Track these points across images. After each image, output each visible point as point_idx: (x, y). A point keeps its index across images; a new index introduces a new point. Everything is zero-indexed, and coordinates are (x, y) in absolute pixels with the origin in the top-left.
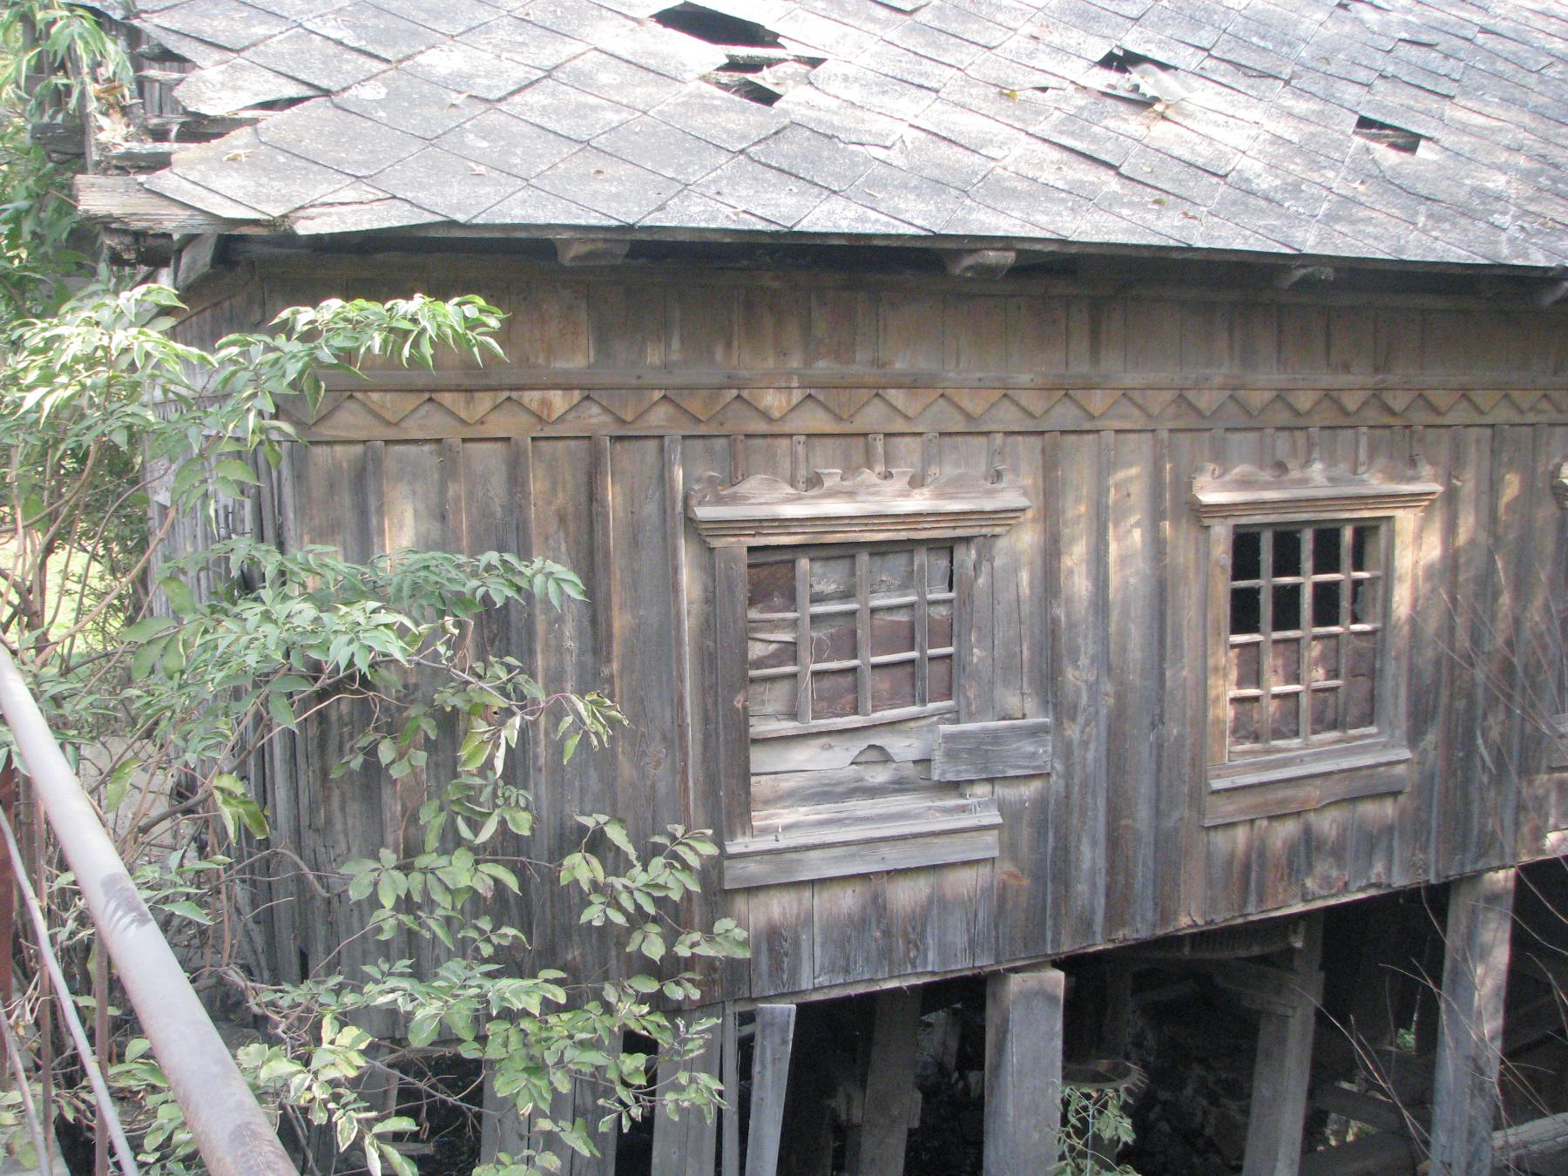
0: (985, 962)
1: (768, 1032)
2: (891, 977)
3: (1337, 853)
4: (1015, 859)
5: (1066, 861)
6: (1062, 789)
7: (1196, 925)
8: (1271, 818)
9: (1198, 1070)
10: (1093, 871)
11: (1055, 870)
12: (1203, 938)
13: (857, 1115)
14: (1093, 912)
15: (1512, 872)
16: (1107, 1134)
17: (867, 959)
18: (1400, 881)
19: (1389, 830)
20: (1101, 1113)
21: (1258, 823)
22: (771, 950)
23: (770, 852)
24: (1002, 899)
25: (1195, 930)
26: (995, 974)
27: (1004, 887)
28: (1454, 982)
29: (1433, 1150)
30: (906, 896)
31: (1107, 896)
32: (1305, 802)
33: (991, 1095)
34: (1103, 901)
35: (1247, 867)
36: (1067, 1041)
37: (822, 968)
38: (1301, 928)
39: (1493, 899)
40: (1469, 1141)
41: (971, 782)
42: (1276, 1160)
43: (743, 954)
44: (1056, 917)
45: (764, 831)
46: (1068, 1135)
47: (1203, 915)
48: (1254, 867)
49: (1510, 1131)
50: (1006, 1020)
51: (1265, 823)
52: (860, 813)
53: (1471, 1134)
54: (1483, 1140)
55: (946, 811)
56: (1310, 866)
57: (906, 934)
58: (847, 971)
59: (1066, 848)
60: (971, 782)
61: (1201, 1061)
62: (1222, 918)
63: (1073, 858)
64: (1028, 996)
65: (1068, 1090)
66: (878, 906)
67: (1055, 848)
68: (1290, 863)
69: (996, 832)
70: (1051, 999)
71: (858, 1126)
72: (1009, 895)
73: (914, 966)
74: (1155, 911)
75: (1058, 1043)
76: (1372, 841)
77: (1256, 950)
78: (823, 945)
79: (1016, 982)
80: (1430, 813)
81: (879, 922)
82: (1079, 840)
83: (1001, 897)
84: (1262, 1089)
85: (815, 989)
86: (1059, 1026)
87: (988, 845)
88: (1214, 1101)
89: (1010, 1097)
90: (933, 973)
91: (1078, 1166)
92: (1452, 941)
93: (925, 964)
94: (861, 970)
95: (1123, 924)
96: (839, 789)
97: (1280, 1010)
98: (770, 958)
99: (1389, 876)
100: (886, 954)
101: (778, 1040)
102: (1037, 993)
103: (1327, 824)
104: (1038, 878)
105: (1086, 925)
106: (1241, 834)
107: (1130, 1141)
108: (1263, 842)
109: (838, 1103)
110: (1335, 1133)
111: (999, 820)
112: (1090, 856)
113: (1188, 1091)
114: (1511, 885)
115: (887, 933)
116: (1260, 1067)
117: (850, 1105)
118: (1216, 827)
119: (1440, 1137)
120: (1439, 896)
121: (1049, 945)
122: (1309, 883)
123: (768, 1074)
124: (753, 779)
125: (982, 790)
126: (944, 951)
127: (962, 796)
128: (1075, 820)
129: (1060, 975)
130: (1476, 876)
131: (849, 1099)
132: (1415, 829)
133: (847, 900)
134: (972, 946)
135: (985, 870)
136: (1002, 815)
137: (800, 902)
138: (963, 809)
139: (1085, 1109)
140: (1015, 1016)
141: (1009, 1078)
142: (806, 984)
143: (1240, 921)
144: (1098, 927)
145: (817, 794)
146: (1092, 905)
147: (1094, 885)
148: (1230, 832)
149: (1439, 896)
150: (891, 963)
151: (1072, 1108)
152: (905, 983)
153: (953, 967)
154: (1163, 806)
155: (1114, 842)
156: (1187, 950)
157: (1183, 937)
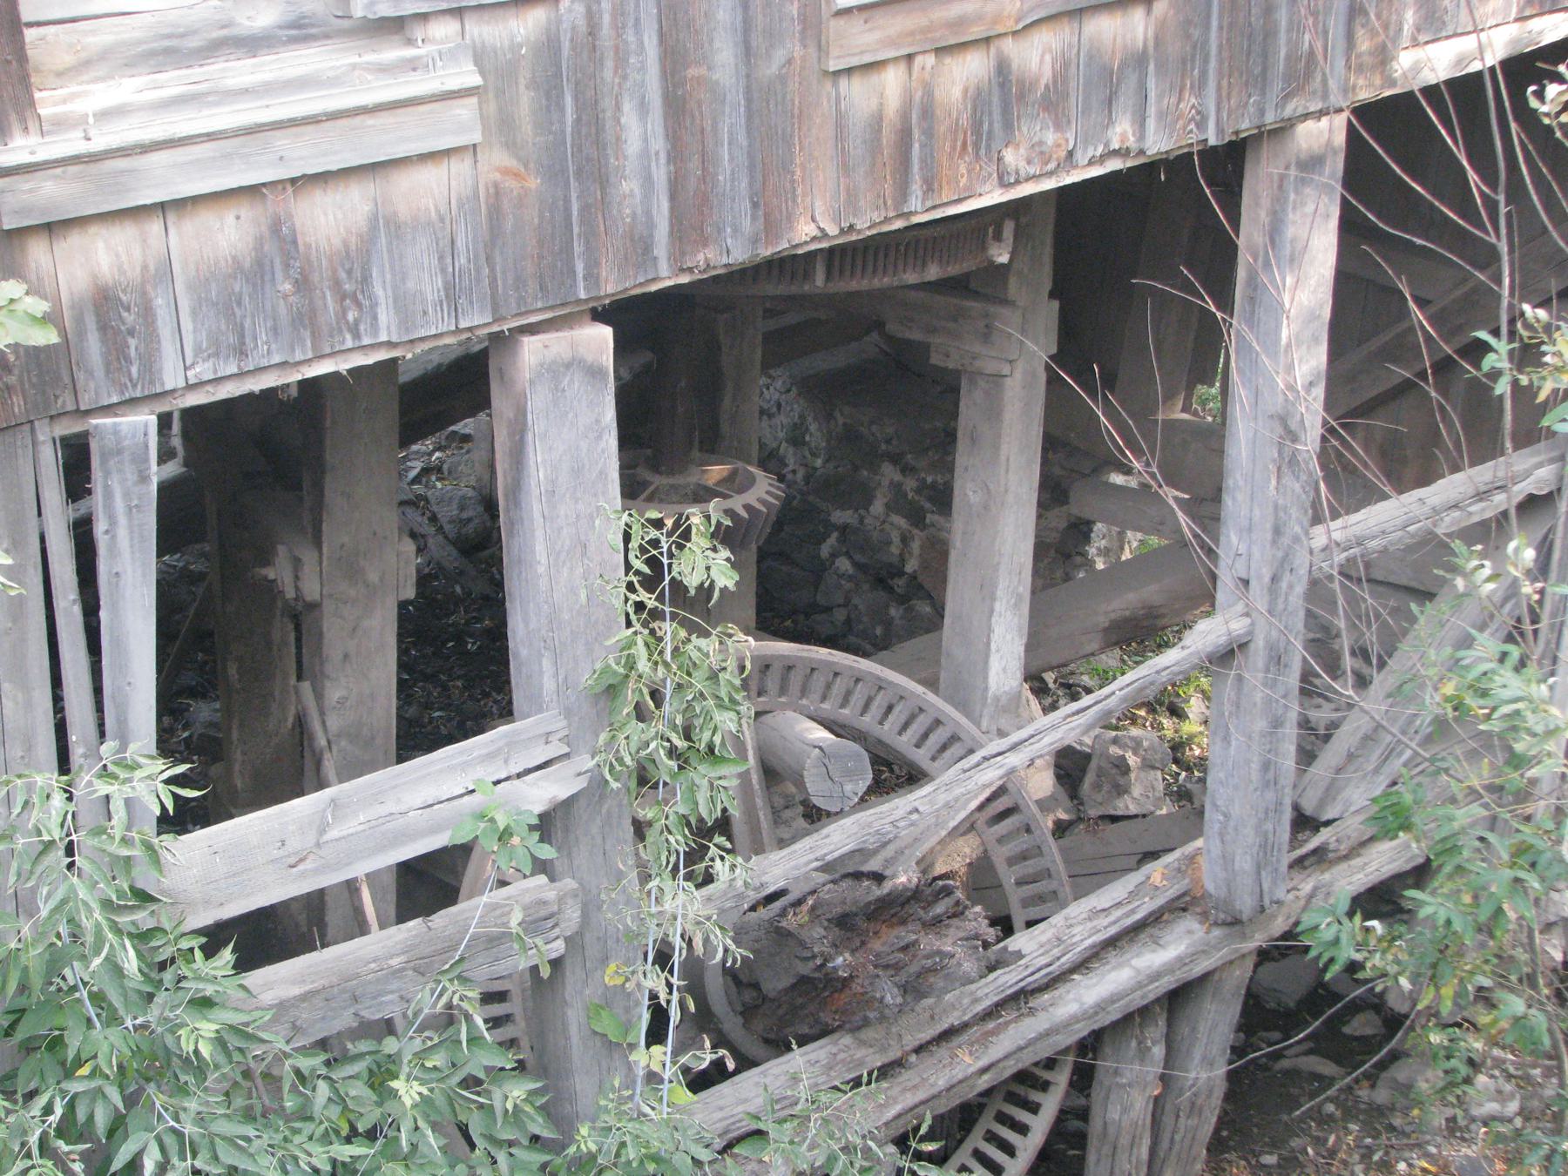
0: (477, 318)
2: (320, 357)
3: (1053, 103)
4: (511, 146)
5: (599, 144)
6: (581, 23)
7: (825, 235)
8: (940, 51)
9: (889, 472)
10: (645, 154)
11: (582, 158)
12: (844, 256)
13: (311, 589)
14: (651, 225)
15: (1340, 121)
16: (692, 581)
17: (275, 330)
18: (1158, 143)
19: (1139, 60)
20: (681, 547)
21: (919, 60)
22: (103, 328)
23: (76, 160)
24: (495, 213)
25: (824, 245)
26: (496, 337)
27: (497, 192)
28: (1252, 300)
29: (1222, 564)
30: (327, 220)
31: (673, 197)
32: (997, 19)
33: (511, 534)
34: (666, 205)
35: (905, 135)
36: (625, 441)
37: (198, 350)
38: (1009, 229)
39: (1312, 163)
40: (1274, 542)
41: (424, 17)
42: (993, 599)
43: (47, 337)
44: (590, 236)
45: (61, 124)
46: (630, 587)
47: (837, 219)
48: (916, 134)
49: (1334, 525)
50: (521, 412)
51: (930, 60)
52: (232, 82)
53: (1277, 531)
54: (1296, 539)
55: (383, 69)
56: (1008, 126)
57: (337, 284)
58: (241, 352)
59: (598, 123)
60: (424, 17)
61: (895, 459)
62: (868, 221)
63: (609, 136)
64: (555, 371)
65: (625, 517)
66: (283, 238)
67: (578, 121)
68: (977, 126)
69: (474, 100)
70: (594, 372)
71: (314, 607)
72: (506, 205)
73: (357, 336)
74: (754, 218)
75: (611, 441)
76: (1108, 82)
77: (933, 272)
78: (194, 313)
79: (532, 351)
80: (1207, 26)
81: (287, 266)
82: (618, 107)
83: (494, 209)
84: (967, 492)
85: (190, 387)
86: (610, 414)
87: (461, 124)
88: (917, 518)
89: (539, 533)
90: (390, 345)
91: (653, 632)
92: (1250, 236)
94: (266, 351)
95: (705, 242)
96: (194, 43)
97: (990, 367)
98: (104, 341)
99: (1141, 136)
100: (306, 319)
101: (131, 476)
102: (568, 366)
103: (1035, 56)
104: (554, 173)
105: (641, 248)
106: (892, 81)
107: (731, 585)
108: (929, 92)
109: (279, 572)
110: (1105, 552)
111: (477, 80)
112: (638, 133)
113: (878, 507)
114: (1340, 139)
115: (303, 284)
116: (962, 458)
117: (297, 571)
118: (849, 71)
119: (1232, 540)
120: (1227, 163)
121: (581, 284)
122: (1010, 156)
123: (122, 532)
124: (30, 34)
125: (444, 30)
126: (402, 305)
127: (410, 42)
128: (608, 73)
129: (606, 332)
130: (1283, 130)
131: (297, 563)
132: (1177, 60)
133: (230, 234)
134: (452, 297)
135: (460, 168)
136: (482, 73)
138: (413, 65)
139: (655, 543)
140: (537, 402)
141: (535, 505)
142: (172, 377)
143: (898, 225)
144: (661, 249)
145: (153, 54)
146: (648, 213)
147: (648, 180)
148: (874, 78)
149: (1227, 163)
150: (316, 337)
151: (634, 544)
152: (343, 365)
153: (423, 333)
154: (757, 40)
155: (677, 108)
156: (820, 279)
157: (811, 255)
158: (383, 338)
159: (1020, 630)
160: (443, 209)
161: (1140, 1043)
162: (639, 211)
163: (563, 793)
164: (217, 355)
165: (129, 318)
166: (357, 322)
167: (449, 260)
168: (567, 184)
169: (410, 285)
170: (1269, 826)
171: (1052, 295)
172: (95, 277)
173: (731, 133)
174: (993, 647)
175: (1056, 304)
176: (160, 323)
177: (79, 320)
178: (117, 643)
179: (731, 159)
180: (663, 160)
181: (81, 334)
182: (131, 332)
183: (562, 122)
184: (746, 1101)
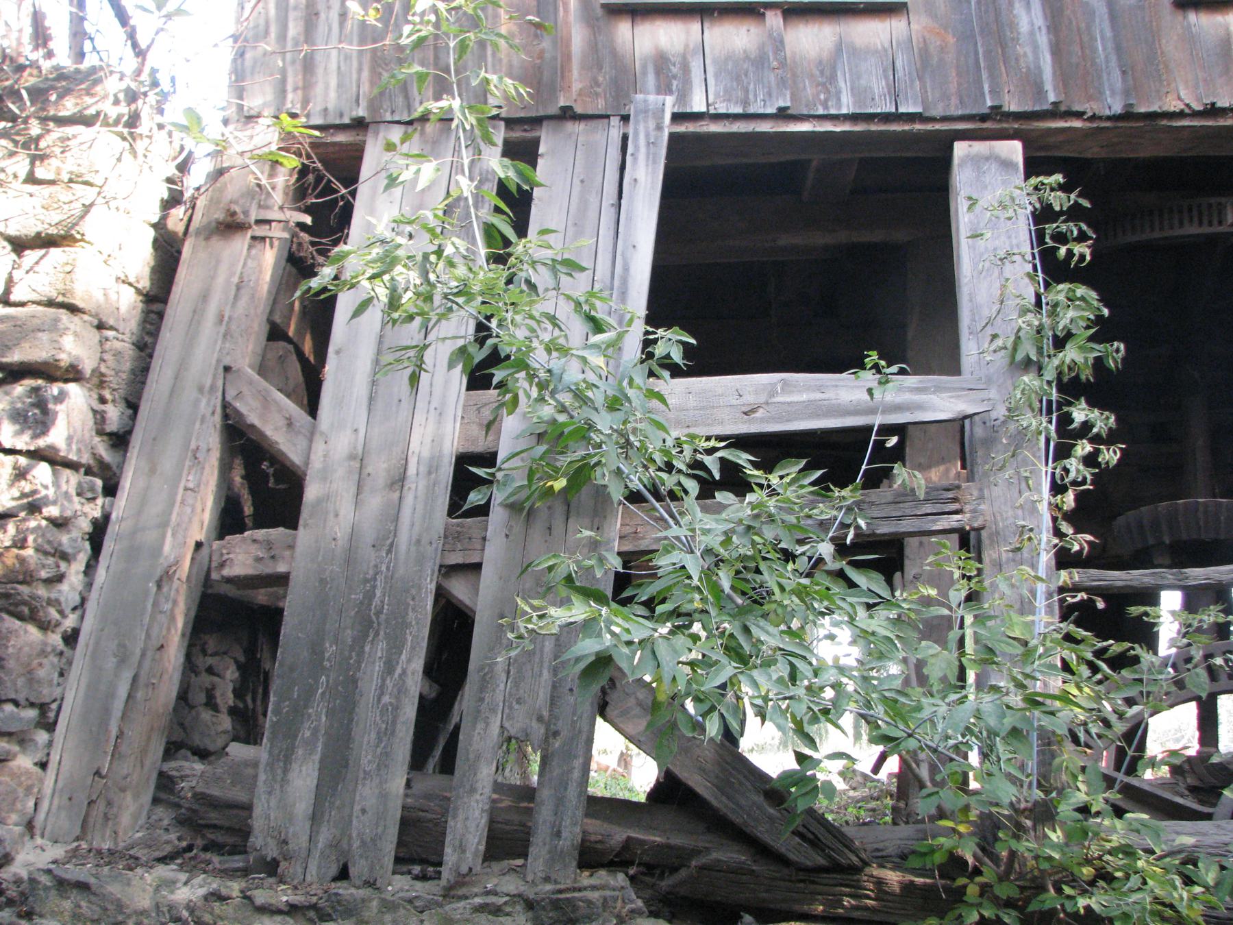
1: (641, 117)
22: (658, 72)
37: (717, 95)
73: (826, 107)
78: (716, 76)
93: (839, 106)
101: (652, 124)
102: (987, 159)
104: (966, 37)
137: (688, 32)
147: (1036, 48)
158: (844, 111)
160: (887, 45)
162: (1032, 66)
163: (971, 410)
164: (729, 100)
165: (674, 70)
166: (826, 100)
167: (891, 73)
168: (976, 44)
169: (863, 82)
172: (657, 48)
173: (1101, 31)
176: (693, 74)
177: (644, 67)
178: (629, 219)
179: (1104, 49)
180: (1044, 30)
181: (645, 73)
182: (675, 77)
183: (970, 8)
184: (1205, 834)
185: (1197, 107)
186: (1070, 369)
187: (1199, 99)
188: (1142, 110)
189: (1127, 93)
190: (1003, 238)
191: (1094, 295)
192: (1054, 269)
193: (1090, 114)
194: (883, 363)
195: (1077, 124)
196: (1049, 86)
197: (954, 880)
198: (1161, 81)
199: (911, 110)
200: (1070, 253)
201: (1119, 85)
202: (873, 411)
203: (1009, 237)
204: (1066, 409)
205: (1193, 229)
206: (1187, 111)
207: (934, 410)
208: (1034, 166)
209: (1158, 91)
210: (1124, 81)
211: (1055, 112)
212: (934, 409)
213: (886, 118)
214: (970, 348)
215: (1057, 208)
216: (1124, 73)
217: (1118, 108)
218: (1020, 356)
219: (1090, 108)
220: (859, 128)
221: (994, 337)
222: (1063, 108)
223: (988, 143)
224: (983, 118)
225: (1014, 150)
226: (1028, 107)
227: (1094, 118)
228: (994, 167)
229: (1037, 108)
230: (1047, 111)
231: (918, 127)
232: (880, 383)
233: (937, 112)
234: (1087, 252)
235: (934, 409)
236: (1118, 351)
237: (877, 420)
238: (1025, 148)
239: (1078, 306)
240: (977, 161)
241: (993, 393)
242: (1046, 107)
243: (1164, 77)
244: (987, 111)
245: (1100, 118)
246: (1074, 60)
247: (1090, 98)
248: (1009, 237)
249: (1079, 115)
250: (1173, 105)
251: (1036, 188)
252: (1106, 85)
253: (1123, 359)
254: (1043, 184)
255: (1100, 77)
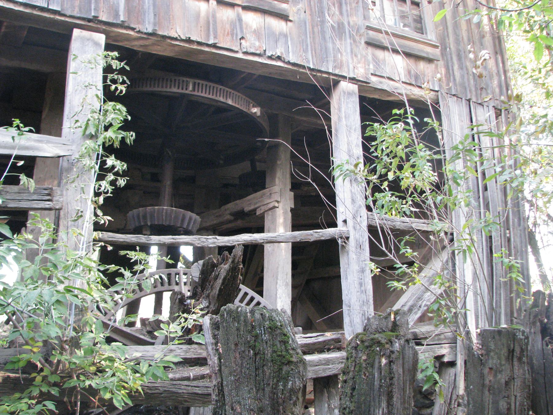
48: (211, 22)
102: (88, 40)
159: (288, 295)
161: (329, 405)
163: (62, 154)
170: (365, 308)
171: (291, 190)
174: (278, 296)
175: (292, 193)
185: (184, 38)
186: (109, 141)
187: (184, 34)
188: (160, 33)
189: (155, 25)
190: (90, 77)
191: (124, 109)
192: (109, 95)
193: (138, 30)
194: (21, 125)
195: (131, 33)
196: (121, 13)
197: (30, 374)
198: (170, 23)
199: (55, 8)
200: (116, 89)
201: (152, 20)
202: (13, 148)
203: (92, 77)
204: (104, 158)
205: (175, 90)
206: (179, 38)
207: (45, 152)
208: (109, 47)
209: (168, 27)
210: (154, 18)
211: (122, 26)
212: (44, 151)
213: (42, 9)
214: (67, 124)
215: (114, 68)
216: (155, 15)
217: (150, 30)
218: (88, 132)
219: (138, 27)
220: (28, 11)
221: (77, 121)
222: (126, 24)
223: (90, 33)
224: (89, 20)
225: (101, 38)
226: (111, 20)
227: (139, 32)
228: (91, 44)
229: (115, 22)
230: (119, 24)
231: (58, 17)
232: (19, 134)
233: (69, 13)
234: (124, 90)
235: (44, 151)
236: (132, 136)
237: (15, 153)
238: (106, 38)
239: (117, 113)
240: (83, 40)
241: (74, 147)
242: (119, 22)
243: (171, 21)
244: (91, 18)
245: (142, 33)
246: (135, 4)
247: (139, 23)
248: (92, 77)
249: (133, 29)
250: (174, 35)
251: (105, 57)
252: (147, 19)
253: (134, 140)
254: (108, 55)
255: (145, 15)
